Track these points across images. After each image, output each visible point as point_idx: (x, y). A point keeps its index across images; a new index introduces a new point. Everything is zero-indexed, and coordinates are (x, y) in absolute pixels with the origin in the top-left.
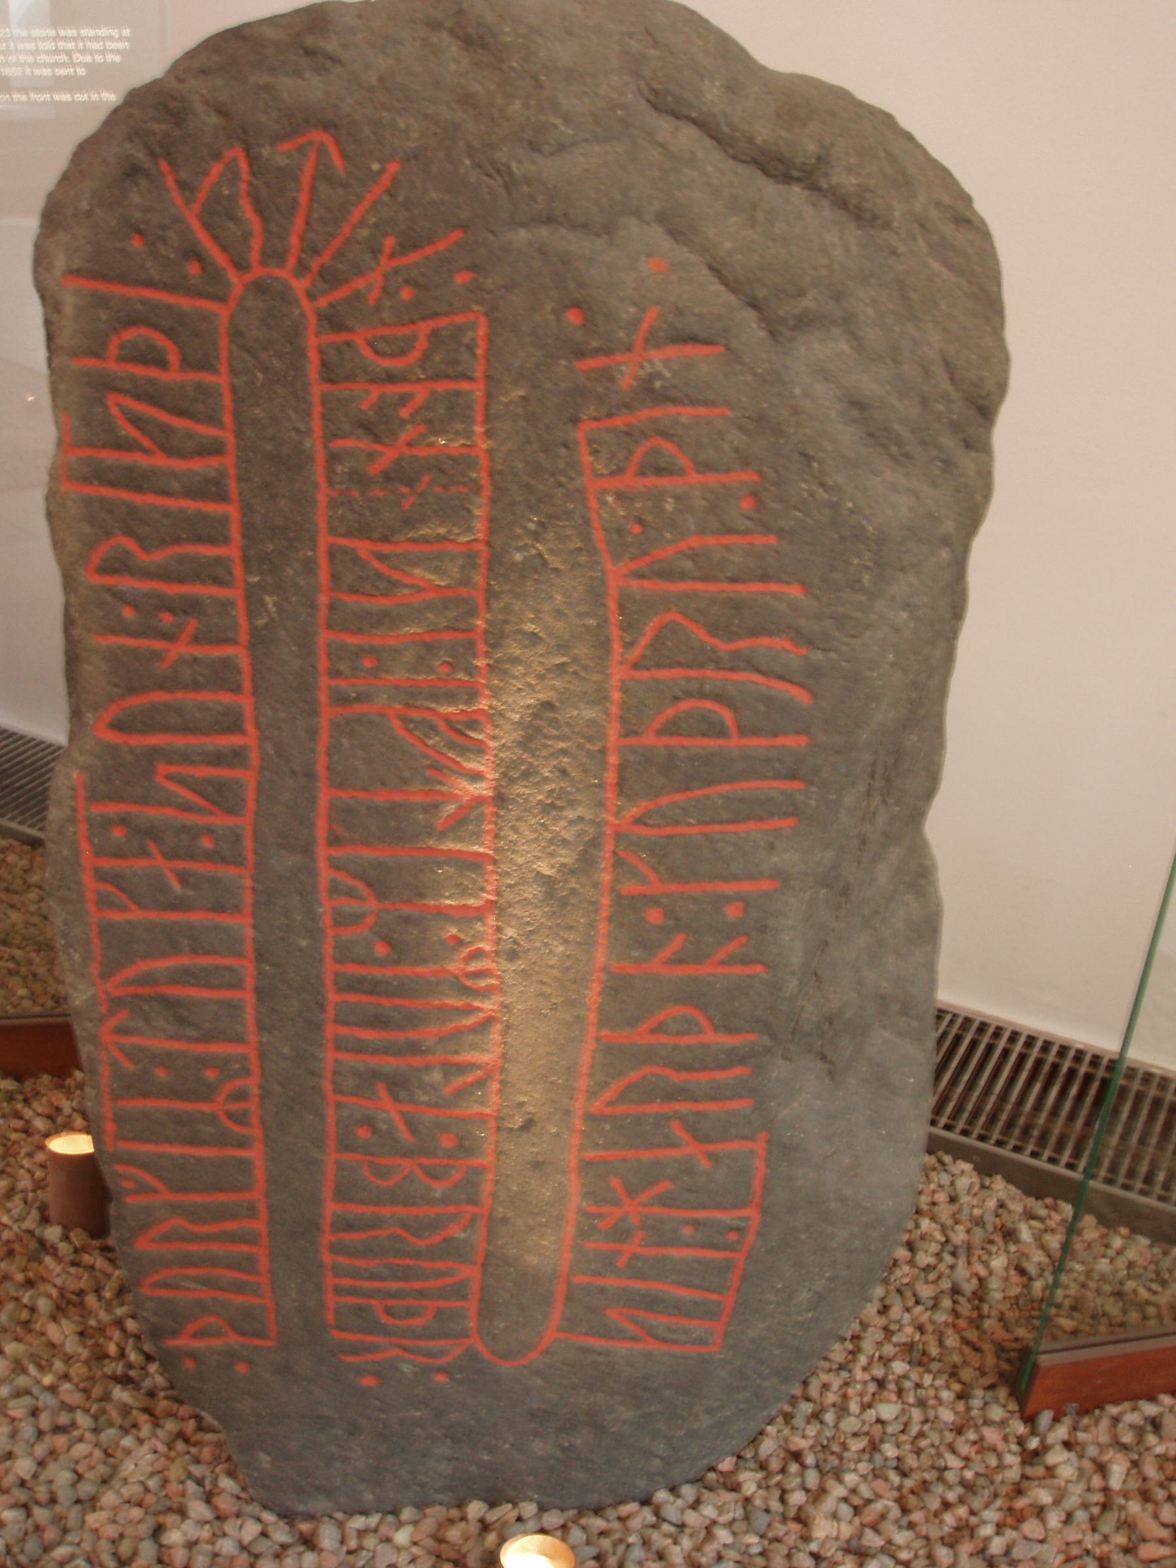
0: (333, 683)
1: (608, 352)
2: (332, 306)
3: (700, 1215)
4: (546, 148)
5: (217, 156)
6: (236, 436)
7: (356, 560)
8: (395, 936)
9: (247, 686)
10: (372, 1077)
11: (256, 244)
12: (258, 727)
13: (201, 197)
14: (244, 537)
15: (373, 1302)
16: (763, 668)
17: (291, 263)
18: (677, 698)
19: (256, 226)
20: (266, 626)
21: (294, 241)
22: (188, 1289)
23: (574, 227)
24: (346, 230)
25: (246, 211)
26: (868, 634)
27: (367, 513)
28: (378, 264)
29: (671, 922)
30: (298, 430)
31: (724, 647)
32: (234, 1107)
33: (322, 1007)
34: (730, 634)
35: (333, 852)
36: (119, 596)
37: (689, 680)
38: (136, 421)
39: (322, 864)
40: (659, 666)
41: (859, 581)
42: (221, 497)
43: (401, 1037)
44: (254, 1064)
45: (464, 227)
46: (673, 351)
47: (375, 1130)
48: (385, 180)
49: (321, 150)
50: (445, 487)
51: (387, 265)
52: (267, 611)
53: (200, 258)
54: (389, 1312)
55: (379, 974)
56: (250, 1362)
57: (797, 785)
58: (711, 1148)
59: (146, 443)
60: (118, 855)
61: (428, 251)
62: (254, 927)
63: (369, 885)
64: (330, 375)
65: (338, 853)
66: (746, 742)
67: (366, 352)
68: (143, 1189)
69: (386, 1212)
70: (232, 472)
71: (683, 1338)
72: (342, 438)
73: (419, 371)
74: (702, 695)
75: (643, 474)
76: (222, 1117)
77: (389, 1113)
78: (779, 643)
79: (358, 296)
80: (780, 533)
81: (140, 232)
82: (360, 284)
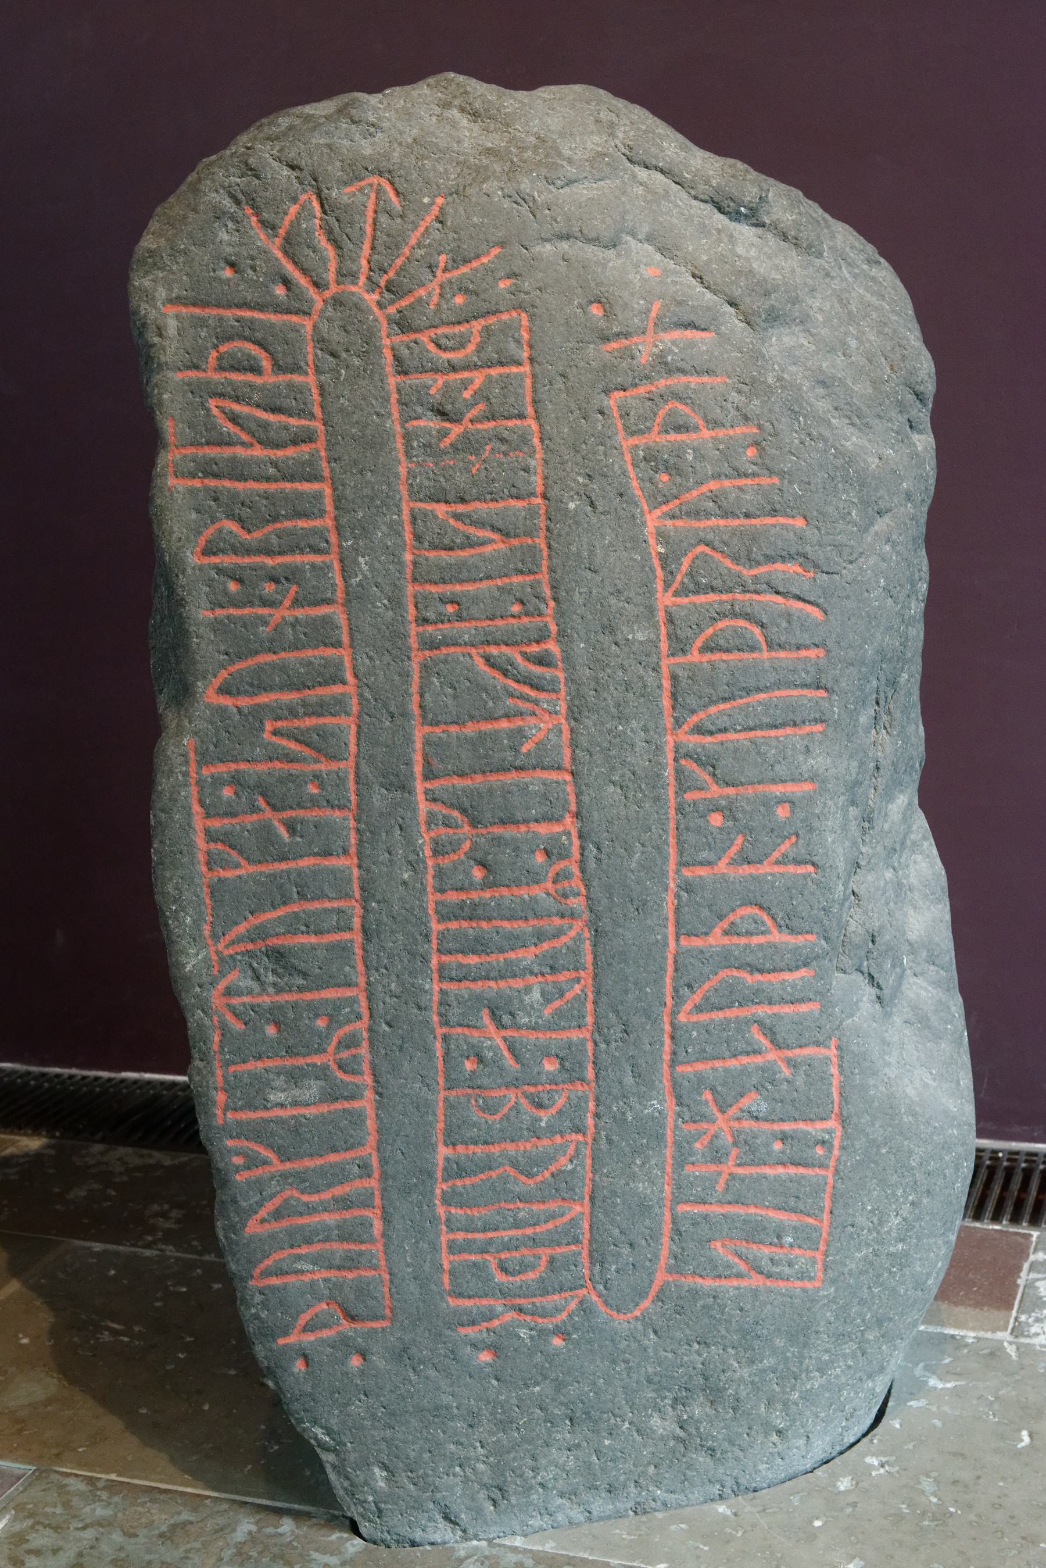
0: (421, 629)
1: (626, 335)
2: (400, 312)
3: (787, 1127)
4: (559, 183)
5: (295, 200)
8: (490, 857)
9: (345, 639)
11: (333, 266)
12: (356, 676)
13: (282, 232)
14: (337, 508)
15: (487, 1257)
16: (781, 590)
17: (362, 280)
19: (330, 252)
20: (360, 584)
21: (364, 263)
22: (302, 1272)
23: (589, 241)
24: (407, 251)
26: (861, 560)
27: (442, 479)
28: (434, 276)
29: (731, 823)
30: (378, 414)
31: (748, 573)
33: (427, 936)
34: (752, 562)
35: (428, 785)
37: (721, 603)
39: (421, 797)
40: (696, 592)
41: (850, 514)
42: (315, 477)
43: (496, 959)
45: (502, 244)
46: (677, 334)
47: (481, 1060)
48: (435, 211)
49: (379, 192)
50: (505, 454)
51: (441, 277)
53: (286, 282)
54: (504, 1269)
56: (363, 1355)
57: (822, 693)
58: (789, 1054)
59: (245, 437)
61: (475, 264)
62: (360, 867)
63: (464, 811)
64: (403, 370)
65: (434, 785)
66: (773, 654)
67: (431, 347)
68: (254, 1162)
69: (495, 1150)
71: (787, 1270)
72: (416, 418)
74: (735, 615)
75: (667, 432)
76: (333, 1067)
77: (493, 1039)
78: (792, 568)
79: (420, 301)
80: (781, 474)
82: (422, 292)
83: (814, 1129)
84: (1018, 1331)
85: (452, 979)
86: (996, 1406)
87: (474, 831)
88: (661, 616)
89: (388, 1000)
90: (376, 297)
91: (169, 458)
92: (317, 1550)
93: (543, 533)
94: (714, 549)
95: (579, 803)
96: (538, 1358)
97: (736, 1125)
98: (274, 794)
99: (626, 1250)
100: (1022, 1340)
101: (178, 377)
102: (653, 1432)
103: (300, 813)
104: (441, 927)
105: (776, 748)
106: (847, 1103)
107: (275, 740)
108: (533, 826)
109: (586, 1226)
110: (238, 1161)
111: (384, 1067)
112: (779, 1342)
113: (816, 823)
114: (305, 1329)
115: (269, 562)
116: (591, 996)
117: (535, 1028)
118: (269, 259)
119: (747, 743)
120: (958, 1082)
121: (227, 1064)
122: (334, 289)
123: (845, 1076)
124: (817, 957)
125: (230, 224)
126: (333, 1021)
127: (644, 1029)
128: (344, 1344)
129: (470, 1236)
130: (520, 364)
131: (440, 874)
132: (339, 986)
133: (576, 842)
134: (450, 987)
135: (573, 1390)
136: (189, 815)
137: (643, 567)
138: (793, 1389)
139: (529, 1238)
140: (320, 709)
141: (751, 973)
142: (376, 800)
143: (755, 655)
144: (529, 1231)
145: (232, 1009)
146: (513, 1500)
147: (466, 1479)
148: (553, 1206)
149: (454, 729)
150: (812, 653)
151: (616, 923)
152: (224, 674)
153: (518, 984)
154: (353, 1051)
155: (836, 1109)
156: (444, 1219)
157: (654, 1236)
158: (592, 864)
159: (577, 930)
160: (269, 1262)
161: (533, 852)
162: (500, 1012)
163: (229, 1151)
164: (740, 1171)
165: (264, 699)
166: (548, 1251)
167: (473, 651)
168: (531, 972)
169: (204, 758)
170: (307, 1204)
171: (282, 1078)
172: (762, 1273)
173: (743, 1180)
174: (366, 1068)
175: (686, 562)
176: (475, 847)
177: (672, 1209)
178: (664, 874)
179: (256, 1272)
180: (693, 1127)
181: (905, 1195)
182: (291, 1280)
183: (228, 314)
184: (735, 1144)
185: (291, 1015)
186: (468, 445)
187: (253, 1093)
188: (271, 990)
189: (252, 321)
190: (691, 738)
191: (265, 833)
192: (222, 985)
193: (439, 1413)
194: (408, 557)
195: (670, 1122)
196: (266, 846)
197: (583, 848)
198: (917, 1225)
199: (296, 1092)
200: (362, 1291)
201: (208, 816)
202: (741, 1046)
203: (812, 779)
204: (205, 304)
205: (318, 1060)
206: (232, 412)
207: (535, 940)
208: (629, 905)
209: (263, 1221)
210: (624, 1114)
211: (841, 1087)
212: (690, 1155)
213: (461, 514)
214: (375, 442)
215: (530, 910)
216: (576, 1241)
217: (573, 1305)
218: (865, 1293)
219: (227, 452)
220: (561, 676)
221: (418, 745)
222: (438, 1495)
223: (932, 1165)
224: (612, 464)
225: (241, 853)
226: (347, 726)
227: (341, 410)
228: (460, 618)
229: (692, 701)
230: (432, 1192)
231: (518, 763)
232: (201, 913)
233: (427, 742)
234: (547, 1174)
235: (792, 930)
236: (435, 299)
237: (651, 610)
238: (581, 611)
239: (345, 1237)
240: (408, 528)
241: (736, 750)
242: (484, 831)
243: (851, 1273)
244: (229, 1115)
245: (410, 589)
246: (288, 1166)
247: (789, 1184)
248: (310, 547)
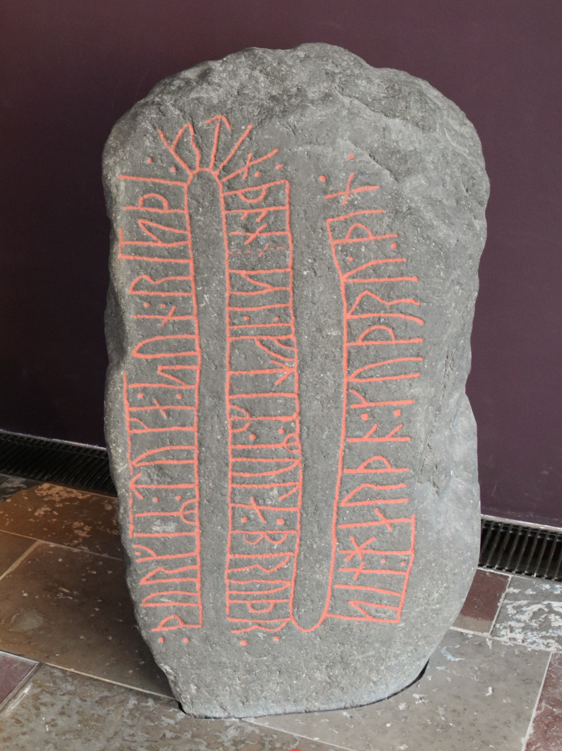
0: (231, 327)
3: (388, 553)
6: (191, 233)
7: (240, 278)
8: (258, 431)
9: (196, 331)
11: (198, 158)
12: (201, 348)
14: (195, 272)
15: (246, 602)
22: (164, 602)
32: (187, 512)
33: (227, 465)
35: (231, 397)
36: (141, 298)
39: (227, 402)
42: (185, 257)
44: (196, 492)
47: (249, 519)
50: (275, 248)
54: (253, 607)
56: (189, 639)
57: (420, 359)
58: (392, 521)
62: (198, 432)
64: (228, 207)
66: (397, 342)
67: (242, 198)
68: (144, 554)
69: (253, 557)
70: (190, 246)
73: (263, 203)
83: (401, 555)
85: (237, 483)
87: (251, 419)
93: (291, 285)
97: (364, 552)
99: (309, 603)
103: (173, 407)
108: (279, 418)
109: (292, 592)
110: (137, 554)
111: (204, 519)
113: (412, 419)
114: (164, 626)
115: (163, 295)
116: (301, 494)
117: (274, 506)
119: (382, 383)
121: (135, 513)
122: (198, 169)
124: (409, 478)
126: (183, 499)
129: (239, 593)
131: (234, 436)
132: (186, 483)
133: (298, 425)
134: (237, 486)
136: (122, 405)
137: (337, 302)
140: (183, 361)
141: (376, 485)
142: (207, 403)
144: (266, 592)
145: (138, 490)
148: (278, 582)
149: (244, 373)
150: (416, 341)
151: (314, 462)
152: (140, 344)
153: (268, 487)
154: (191, 511)
156: (228, 585)
157: (322, 598)
158: (305, 435)
160: (149, 597)
161: (277, 429)
163: (134, 550)
164: (365, 572)
165: (158, 356)
166: (274, 601)
167: (255, 338)
168: (274, 482)
169: (130, 381)
170: (167, 574)
171: (159, 521)
173: (365, 576)
174: (196, 518)
176: (251, 426)
178: (338, 441)
179: (144, 601)
180: (344, 552)
182: (158, 605)
184: (363, 560)
185: (164, 494)
187: (145, 526)
188: (156, 483)
191: (156, 414)
192: (134, 479)
194: (227, 295)
195: (333, 550)
196: (156, 421)
197: (301, 428)
200: (190, 612)
201: (131, 406)
203: (412, 399)
205: (175, 514)
209: (148, 580)
214: (214, 243)
215: (275, 453)
217: (284, 625)
220: (296, 351)
225: (145, 423)
226: (196, 368)
227: (199, 227)
228: (250, 323)
230: (223, 573)
231: (273, 389)
233: (232, 378)
234: (276, 569)
235: (397, 467)
236: (245, 175)
237: (340, 321)
240: (227, 281)
242: (256, 419)
244: (135, 534)
246: (160, 558)
248: (183, 290)
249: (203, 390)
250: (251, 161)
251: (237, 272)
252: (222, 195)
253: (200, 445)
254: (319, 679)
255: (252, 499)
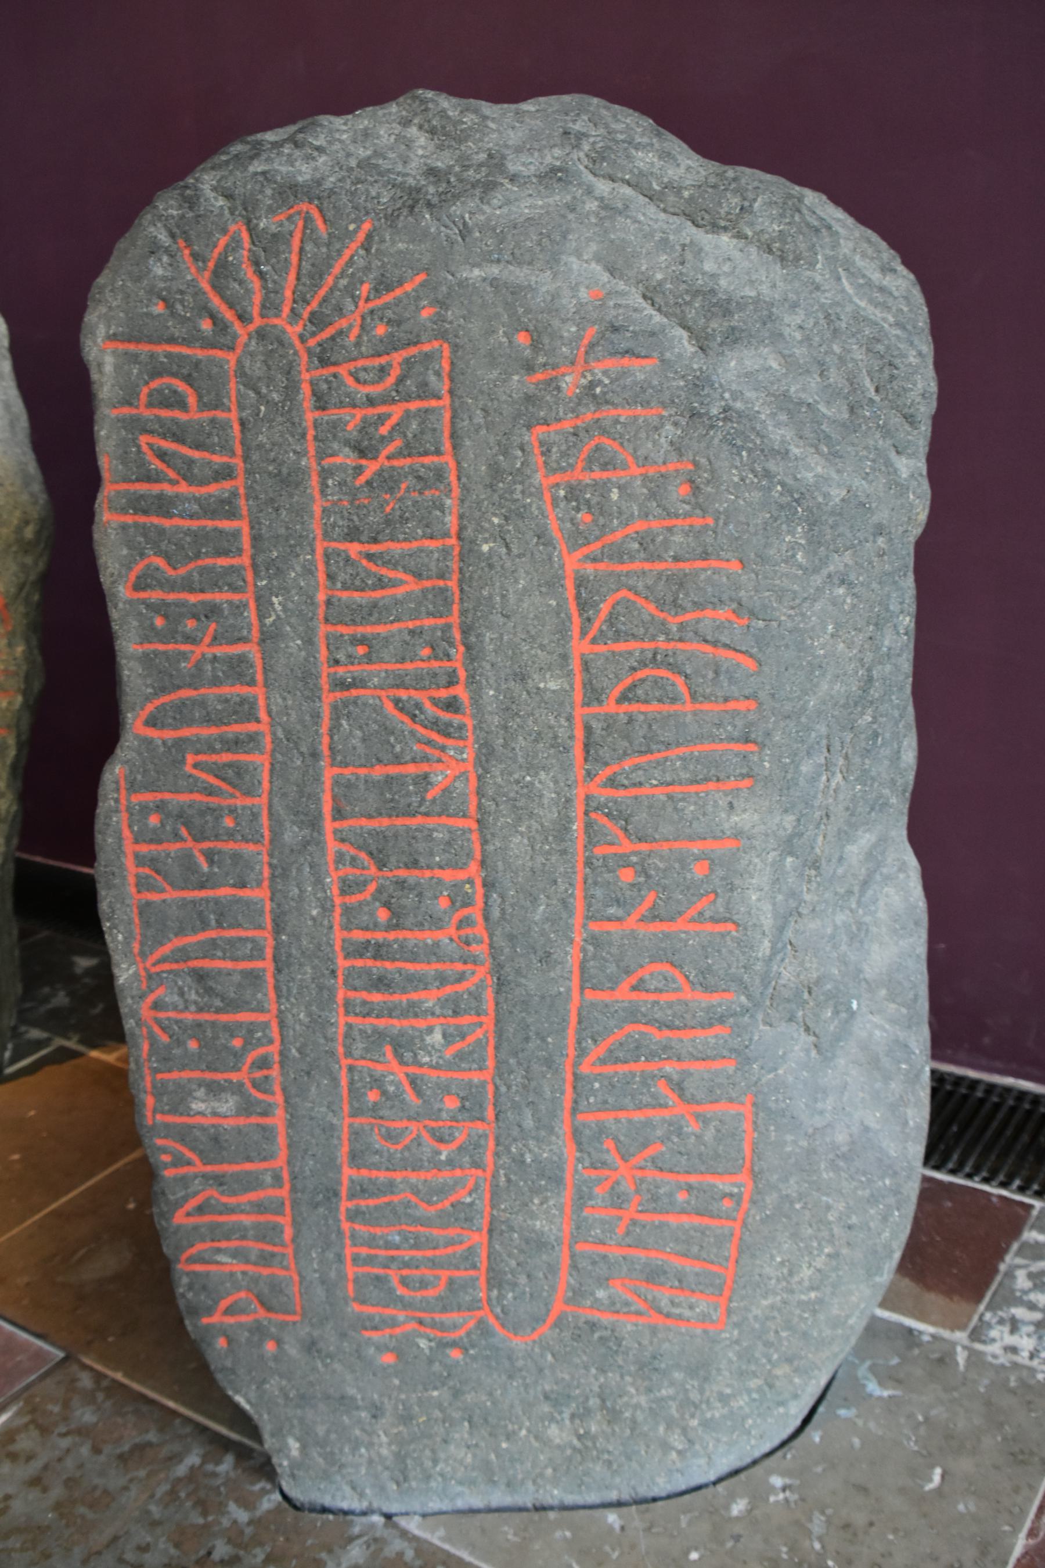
0: (332, 670)
3: (693, 1180)
5: (224, 231)
6: (245, 462)
7: (347, 560)
8: (393, 900)
9: (259, 677)
10: (379, 1037)
11: (257, 299)
12: (269, 713)
14: (253, 547)
15: (389, 1272)
16: (709, 638)
18: (634, 669)
19: (255, 284)
20: (274, 623)
21: (288, 294)
22: (222, 1264)
24: (330, 280)
25: (247, 272)
27: (355, 518)
35: (337, 825)
38: (162, 455)
39: (329, 837)
42: (232, 515)
43: (401, 999)
44: (274, 1032)
47: (384, 1093)
48: (361, 236)
49: (308, 219)
50: (421, 493)
52: (274, 610)
54: (404, 1282)
55: (379, 936)
56: (279, 1342)
59: (172, 475)
60: (156, 839)
62: (272, 900)
64: (321, 402)
66: (698, 706)
67: (350, 381)
68: (179, 1161)
69: (398, 1177)
70: (242, 491)
71: (687, 1313)
72: (332, 455)
76: (248, 1085)
81: (164, 300)
82: (343, 324)
83: (723, 1185)
84: (976, 1335)
85: (356, 1015)
86: (922, 1431)
87: (380, 874)
88: (575, 665)
89: (298, 1027)
90: (298, 329)
91: (108, 491)
92: (237, 1501)
93: (455, 576)
94: (636, 594)
95: (483, 851)
96: (436, 1367)
97: (639, 1174)
98: (197, 824)
99: (523, 1279)
100: (978, 1346)
101: (113, 414)
102: (551, 1441)
103: (219, 845)
104: (348, 963)
105: (695, 803)
106: (759, 1159)
107: (195, 773)
108: (438, 873)
109: (484, 1255)
111: (293, 1090)
112: (678, 1375)
114: (227, 1312)
115: (192, 599)
116: (492, 1042)
117: (436, 1067)
118: (198, 293)
119: (663, 798)
120: (906, 1123)
121: (156, 1071)
122: (258, 322)
123: (760, 1133)
124: (734, 1014)
125: (165, 259)
126: (249, 1043)
127: (544, 1077)
128: (259, 1331)
129: (373, 1252)
130: (439, 398)
131: (347, 911)
132: (253, 1010)
133: (480, 890)
135: (469, 1398)
136: (120, 839)
137: (558, 614)
138: (693, 1416)
139: (429, 1259)
140: (236, 744)
141: (659, 1029)
142: (287, 837)
143: (673, 709)
144: (430, 1254)
145: (158, 1022)
146: (414, 1484)
147: (370, 1462)
148: (452, 1233)
149: (362, 772)
150: (742, 706)
151: (518, 972)
152: (150, 707)
153: (421, 1024)
154: (265, 1072)
155: (748, 1164)
156: (348, 1234)
157: (552, 1269)
158: (496, 913)
159: (479, 976)
160: (193, 1251)
161: (436, 898)
162: (401, 1045)
163: (159, 1149)
164: (643, 1218)
165: (186, 732)
166: (448, 1273)
167: (383, 693)
168: (433, 1014)
169: (133, 787)
170: (225, 1205)
171: (203, 1090)
172: (661, 1313)
173: (644, 1227)
174: (277, 1088)
175: (605, 608)
176: (380, 890)
177: (570, 1247)
178: (569, 927)
179: (184, 1257)
180: (594, 1175)
181: (820, 1248)
182: (212, 1268)
183: (161, 350)
184: (637, 1191)
185: (209, 1034)
186: (387, 481)
187: (179, 1100)
188: (193, 1008)
189: (181, 357)
190: (603, 791)
191: (187, 863)
192: (150, 999)
193: (344, 1402)
194: (321, 597)
195: (568, 1168)
196: (190, 876)
197: (487, 897)
198: (834, 1275)
199: (216, 1104)
200: (276, 1287)
201: (136, 842)
202: (646, 1099)
204: (138, 341)
205: (234, 1077)
206: (159, 448)
207: (437, 983)
208: (532, 956)
209: (188, 1214)
210: (522, 1155)
211: (753, 1143)
212: (590, 1199)
213: (373, 555)
214: (290, 480)
215: (434, 952)
216: (474, 1267)
217: (472, 1324)
218: (771, 1337)
219: (155, 489)
220: (470, 723)
221: (328, 785)
222: (344, 1471)
223: (854, 1220)
224: (530, 504)
225: (165, 878)
226: (259, 761)
227: (260, 446)
228: (370, 661)
229: (605, 753)
230: (337, 1209)
231: (423, 809)
232: (131, 932)
233: (336, 783)
234: (447, 1204)
235: (707, 989)
236: (356, 331)
237: (564, 657)
238: (492, 657)
239: (261, 1238)
240: (321, 567)
241: (650, 807)
242: (390, 875)
243: (756, 1317)
244: (158, 1117)
245: (322, 629)
246: (209, 1169)
247: (692, 1233)
248: (230, 585)
249: (280, 809)
250: (367, 300)
251: (341, 546)
252: (306, 376)
253: (278, 928)
254: (557, 1441)
255: (388, 1050)
